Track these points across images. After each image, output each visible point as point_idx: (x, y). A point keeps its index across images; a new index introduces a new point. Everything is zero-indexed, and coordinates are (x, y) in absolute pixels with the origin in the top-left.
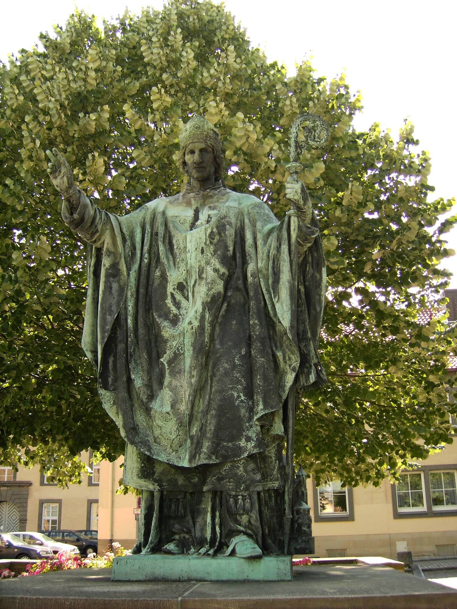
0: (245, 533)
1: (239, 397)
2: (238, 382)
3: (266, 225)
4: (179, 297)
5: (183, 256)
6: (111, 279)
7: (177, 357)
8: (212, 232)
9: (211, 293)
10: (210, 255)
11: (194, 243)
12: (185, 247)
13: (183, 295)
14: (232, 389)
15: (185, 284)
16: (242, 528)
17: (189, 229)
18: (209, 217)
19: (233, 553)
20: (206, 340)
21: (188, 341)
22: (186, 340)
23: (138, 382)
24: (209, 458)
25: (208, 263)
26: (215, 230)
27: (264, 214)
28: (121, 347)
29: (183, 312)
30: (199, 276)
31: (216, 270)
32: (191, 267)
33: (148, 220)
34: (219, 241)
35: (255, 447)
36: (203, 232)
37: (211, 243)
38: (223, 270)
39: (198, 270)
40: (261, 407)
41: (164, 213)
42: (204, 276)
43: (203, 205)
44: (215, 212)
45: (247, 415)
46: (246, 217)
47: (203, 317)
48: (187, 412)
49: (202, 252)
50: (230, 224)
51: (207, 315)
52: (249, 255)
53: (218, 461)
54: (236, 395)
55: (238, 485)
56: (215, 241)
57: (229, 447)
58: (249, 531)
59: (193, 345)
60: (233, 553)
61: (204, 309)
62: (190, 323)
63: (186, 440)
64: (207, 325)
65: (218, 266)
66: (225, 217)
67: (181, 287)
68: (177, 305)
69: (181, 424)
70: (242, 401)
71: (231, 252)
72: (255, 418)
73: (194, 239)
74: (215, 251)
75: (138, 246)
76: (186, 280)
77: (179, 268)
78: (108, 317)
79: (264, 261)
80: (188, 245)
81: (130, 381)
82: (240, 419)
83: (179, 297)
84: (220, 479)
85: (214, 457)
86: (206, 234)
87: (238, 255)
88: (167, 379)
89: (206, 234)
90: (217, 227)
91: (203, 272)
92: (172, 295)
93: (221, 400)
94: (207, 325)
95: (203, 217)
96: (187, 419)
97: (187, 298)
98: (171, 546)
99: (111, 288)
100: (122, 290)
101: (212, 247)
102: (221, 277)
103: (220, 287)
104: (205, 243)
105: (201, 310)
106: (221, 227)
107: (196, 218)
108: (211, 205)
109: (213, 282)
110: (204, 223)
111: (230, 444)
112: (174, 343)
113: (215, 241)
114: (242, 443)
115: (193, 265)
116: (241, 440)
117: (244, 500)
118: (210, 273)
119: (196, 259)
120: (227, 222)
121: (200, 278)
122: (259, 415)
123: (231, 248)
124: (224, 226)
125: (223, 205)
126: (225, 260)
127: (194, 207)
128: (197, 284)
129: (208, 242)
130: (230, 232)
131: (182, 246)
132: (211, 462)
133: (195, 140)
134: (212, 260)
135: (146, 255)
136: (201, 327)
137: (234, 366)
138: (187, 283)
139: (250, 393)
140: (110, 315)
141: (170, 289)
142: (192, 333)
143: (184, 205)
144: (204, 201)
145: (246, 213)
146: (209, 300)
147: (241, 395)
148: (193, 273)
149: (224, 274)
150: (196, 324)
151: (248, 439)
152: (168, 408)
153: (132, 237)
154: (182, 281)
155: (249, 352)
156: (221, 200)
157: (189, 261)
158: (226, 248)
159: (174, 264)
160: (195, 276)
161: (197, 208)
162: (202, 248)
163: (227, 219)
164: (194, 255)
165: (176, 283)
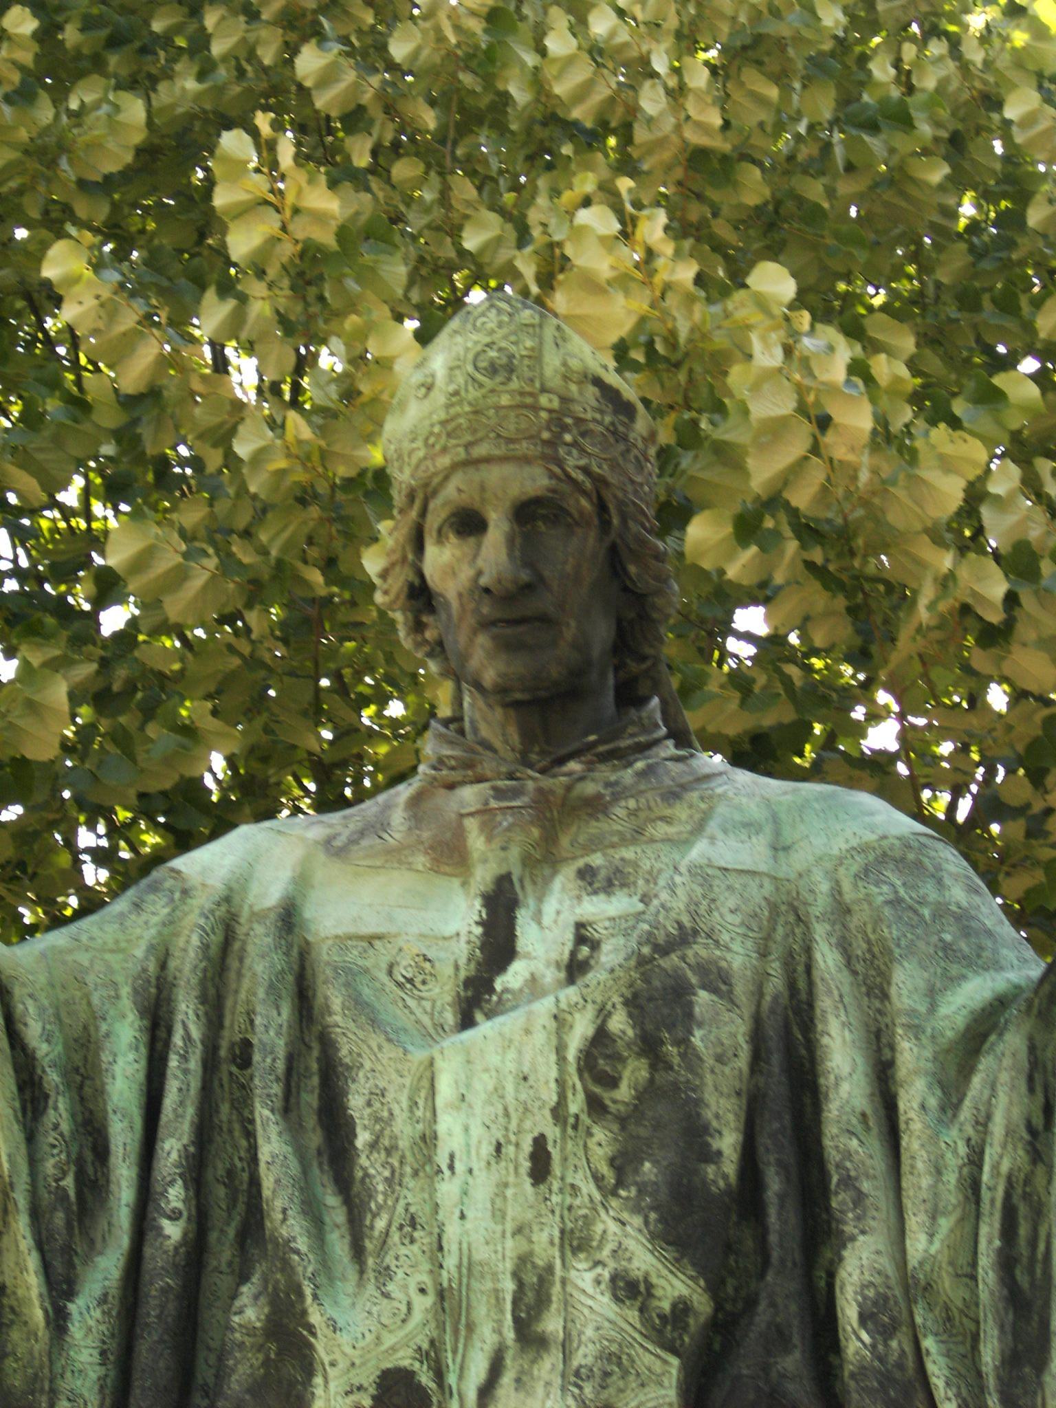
3: (953, 981)
5: (412, 1195)
8: (601, 1037)
10: (588, 1188)
11: (481, 1110)
12: (428, 1140)
15: (425, 1379)
17: (450, 1018)
18: (580, 939)
25: (576, 1241)
26: (619, 1023)
27: (941, 911)
31: (629, 1289)
32: (469, 1267)
34: (647, 1093)
37: (595, 1106)
38: (674, 1286)
39: (509, 1286)
41: (288, 918)
42: (552, 1324)
43: (543, 859)
44: (619, 904)
46: (820, 931)
50: (717, 979)
52: (848, 1182)
56: (624, 1092)
65: (643, 1259)
66: (685, 937)
71: (730, 1167)
73: (483, 1084)
74: (623, 1164)
75: (123, 1135)
76: (433, 1356)
77: (385, 1273)
79: (945, 1224)
80: (448, 1125)
86: (560, 1050)
87: (774, 1184)
89: (560, 1050)
90: (633, 1003)
91: (542, 1301)
95: (541, 938)
101: (600, 1134)
102: (667, 1328)
104: (558, 1113)
106: (661, 999)
107: (498, 945)
108: (597, 860)
109: (614, 1363)
110: (550, 976)
113: (624, 1092)
115: (482, 1253)
118: (589, 1307)
119: (499, 1214)
120: (703, 969)
121: (529, 1337)
123: (728, 1142)
124: (679, 992)
125: (668, 855)
126: (685, 1221)
127: (483, 876)
128: (507, 1379)
129: (576, 1105)
130: (720, 1035)
131: (404, 1130)
133: (481, 450)
134: (606, 1224)
135: (175, 1196)
138: (439, 1375)
143: (421, 861)
144: (550, 839)
145: (820, 904)
148: (481, 1310)
149: (682, 1309)
153: (85, 1075)
154: (404, 1359)
156: (662, 829)
157: (453, 1231)
158: (695, 1138)
159: (358, 1252)
160: (491, 1328)
162: (540, 1142)
163: (700, 950)
165: (367, 1377)
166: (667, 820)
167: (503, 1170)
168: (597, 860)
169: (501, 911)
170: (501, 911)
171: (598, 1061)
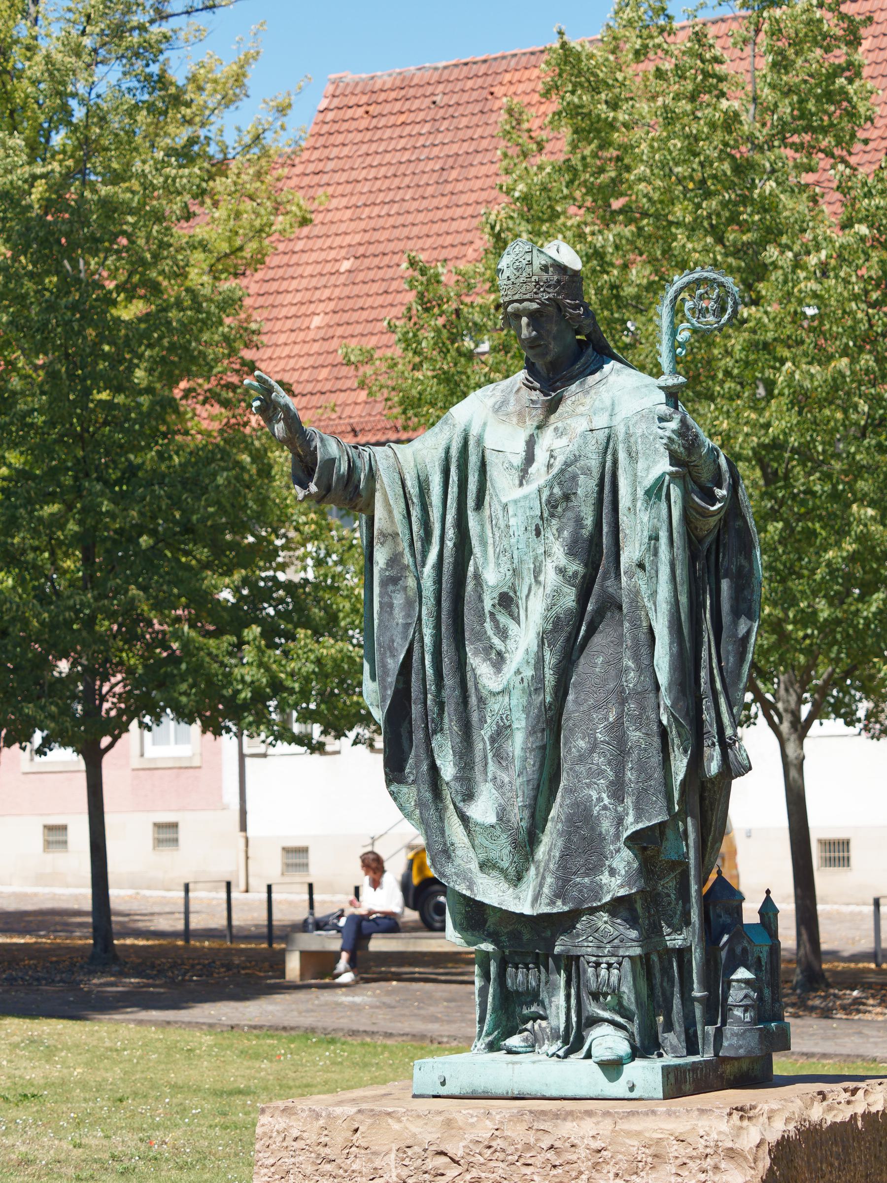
1: (600, 799)
2: (601, 773)
6: (391, 588)
7: (502, 732)
8: (551, 494)
9: (553, 613)
10: (551, 538)
13: (511, 615)
14: (589, 786)
16: (606, 1015)
17: (517, 482)
18: (552, 456)
19: (588, 1056)
21: (517, 700)
22: (514, 702)
23: (448, 770)
24: (552, 903)
26: (557, 490)
28: (416, 710)
29: (511, 644)
30: (536, 577)
31: (561, 571)
33: (454, 453)
35: (621, 886)
36: (535, 495)
40: (630, 819)
41: (480, 441)
42: (541, 578)
45: (612, 831)
47: (540, 661)
48: (524, 824)
49: (538, 534)
50: (587, 471)
51: (547, 655)
53: (566, 909)
54: (595, 796)
57: (584, 885)
58: (618, 1019)
59: (526, 709)
60: (588, 1056)
62: (518, 672)
66: (577, 459)
67: (506, 601)
68: (503, 634)
69: (516, 845)
70: (605, 808)
71: (590, 528)
72: (625, 835)
74: (560, 531)
78: (389, 661)
80: (512, 521)
81: (434, 770)
82: (602, 838)
85: (559, 903)
87: (605, 529)
88: (492, 767)
92: (492, 614)
93: (572, 806)
98: (515, 1041)
99: (391, 606)
103: (569, 599)
104: (541, 517)
105: (535, 649)
107: (530, 458)
108: (560, 424)
111: (586, 880)
112: (496, 707)
113: (559, 509)
114: (605, 878)
116: (602, 873)
118: (550, 577)
119: (528, 546)
120: (582, 468)
122: (629, 832)
123: (589, 522)
124: (574, 478)
130: (586, 486)
132: (555, 911)
136: (539, 678)
137: (594, 747)
139: (618, 790)
140: (393, 656)
141: (488, 604)
142: (523, 690)
143: (515, 420)
145: (621, 436)
146: (550, 627)
147: (604, 796)
148: (525, 572)
149: (575, 574)
150: (529, 672)
151: (613, 872)
154: (505, 589)
155: (620, 718)
157: (516, 553)
158: (579, 521)
161: (532, 436)
163: (582, 463)
164: (523, 538)
165: (496, 595)
166: (582, 404)
167: (528, 534)
168: (560, 424)
169: (531, 444)
171: (552, 504)
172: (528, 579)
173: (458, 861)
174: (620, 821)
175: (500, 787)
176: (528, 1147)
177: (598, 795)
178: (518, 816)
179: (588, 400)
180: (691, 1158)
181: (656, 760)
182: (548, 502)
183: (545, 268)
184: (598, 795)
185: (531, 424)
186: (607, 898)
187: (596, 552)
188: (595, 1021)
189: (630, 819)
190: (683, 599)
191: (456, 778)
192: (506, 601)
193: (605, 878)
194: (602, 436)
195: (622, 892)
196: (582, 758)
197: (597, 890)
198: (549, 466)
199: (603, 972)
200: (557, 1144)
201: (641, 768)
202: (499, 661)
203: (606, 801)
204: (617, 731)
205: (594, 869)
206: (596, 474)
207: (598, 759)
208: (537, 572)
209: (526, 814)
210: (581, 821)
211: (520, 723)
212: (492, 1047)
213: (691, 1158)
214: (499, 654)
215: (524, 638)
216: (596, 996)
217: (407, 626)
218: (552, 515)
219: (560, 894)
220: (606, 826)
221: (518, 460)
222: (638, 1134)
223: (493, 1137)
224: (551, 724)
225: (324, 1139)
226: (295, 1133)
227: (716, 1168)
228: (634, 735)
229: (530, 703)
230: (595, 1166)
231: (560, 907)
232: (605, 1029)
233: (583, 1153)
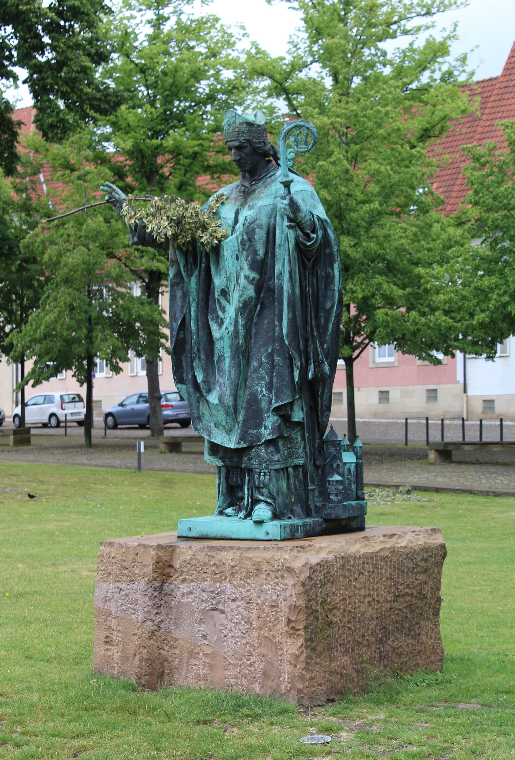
0: (266, 502)
1: (262, 391)
2: (263, 378)
4: (223, 302)
6: (176, 288)
7: (221, 357)
8: (243, 239)
9: (243, 298)
11: (229, 251)
13: (226, 299)
14: (257, 385)
20: (241, 341)
23: (200, 378)
24: (239, 443)
26: (245, 237)
31: (246, 277)
32: (230, 273)
34: (250, 246)
35: (269, 434)
36: (235, 240)
37: (243, 249)
38: (254, 275)
43: (243, 205)
45: (266, 407)
48: (231, 404)
49: (237, 259)
50: (260, 226)
51: (240, 320)
55: (261, 465)
58: (269, 500)
59: (231, 347)
61: (237, 315)
62: (227, 328)
63: (234, 426)
64: (241, 329)
66: (255, 220)
69: (227, 413)
70: (264, 396)
74: (247, 257)
78: (174, 324)
81: (194, 377)
83: (223, 302)
84: (250, 459)
85: (242, 443)
90: (247, 233)
94: (241, 329)
96: (231, 410)
97: (229, 302)
98: (229, 511)
99: (175, 296)
100: (185, 295)
101: (245, 253)
102: (251, 281)
103: (251, 292)
105: (234, 316)
107: (236, 221)
108: (251, 203)
109: (245, 287)
114: (263, 431)
117: (265, 476)
124: (254, 230)
126: (253, 267)
130: (260, 235)
132: (240, 447)
137: (261, 364)
140: (176, 322)
146: (241, 305)
149: (254, 279)
150: (231, 329)
151: (266, 428)
152: (217, 402)
158: (255, 252)
161: (238, 210)
163: (257, 222)
164: (231, 262)
168: (251, 203)
169: (237, 214)
170: (237, 214)
171: (243, 243)
172: (234, 282)
173: (205, 422)
174: (270, 403)
175: (220, 386)
176: (205, 564)
177: (261, 389)
178: (228, 400)
179: (265, 191)
180: (272, 571)
181: (286, 372)
182: (241, 243)
183: (241, 124)
184: (261, 389)
185: (238, 203)
186: (263, 441)
187: (263, 267)
188: (259, 501)
189: (273, 401)
190: (297, 291)
191: (203, 381)
192: (224, 293)
193: (263, 431)
194: (269, 208)
195: (269, 438)
196: (255, 371)
197: (259, 436)
198: (244, 224)
199: (262, 477)
200: (217, 563)
201: (279, 375)
202: (221, 323)
203: (265, 392)
204: (270, 356)
205: (259, 426)
206: (265, 228)
207: (262, 371)
208: (238, 278)
209: (232, 399)
210: (254, 400)
211: (228, 354)
212: (221, 513)
213: (272, 571)
214: (222, 319)
215: (230, 312)
216: (258, 488)
217: (182, 307)
218: (243, 249)
219: (242, 438)
220: (264, 404)
221: (231, 222)
222: (251, 558)
223: (192, 559)
224: (243, 354)
225: (124, 558)
226: (113, 555)
227: (283, 576)
228: (277, 359)
229: (232, 344)
230: (233, 574)
231: (243, 445)
232: (262, 505)
233: (227, 567)
